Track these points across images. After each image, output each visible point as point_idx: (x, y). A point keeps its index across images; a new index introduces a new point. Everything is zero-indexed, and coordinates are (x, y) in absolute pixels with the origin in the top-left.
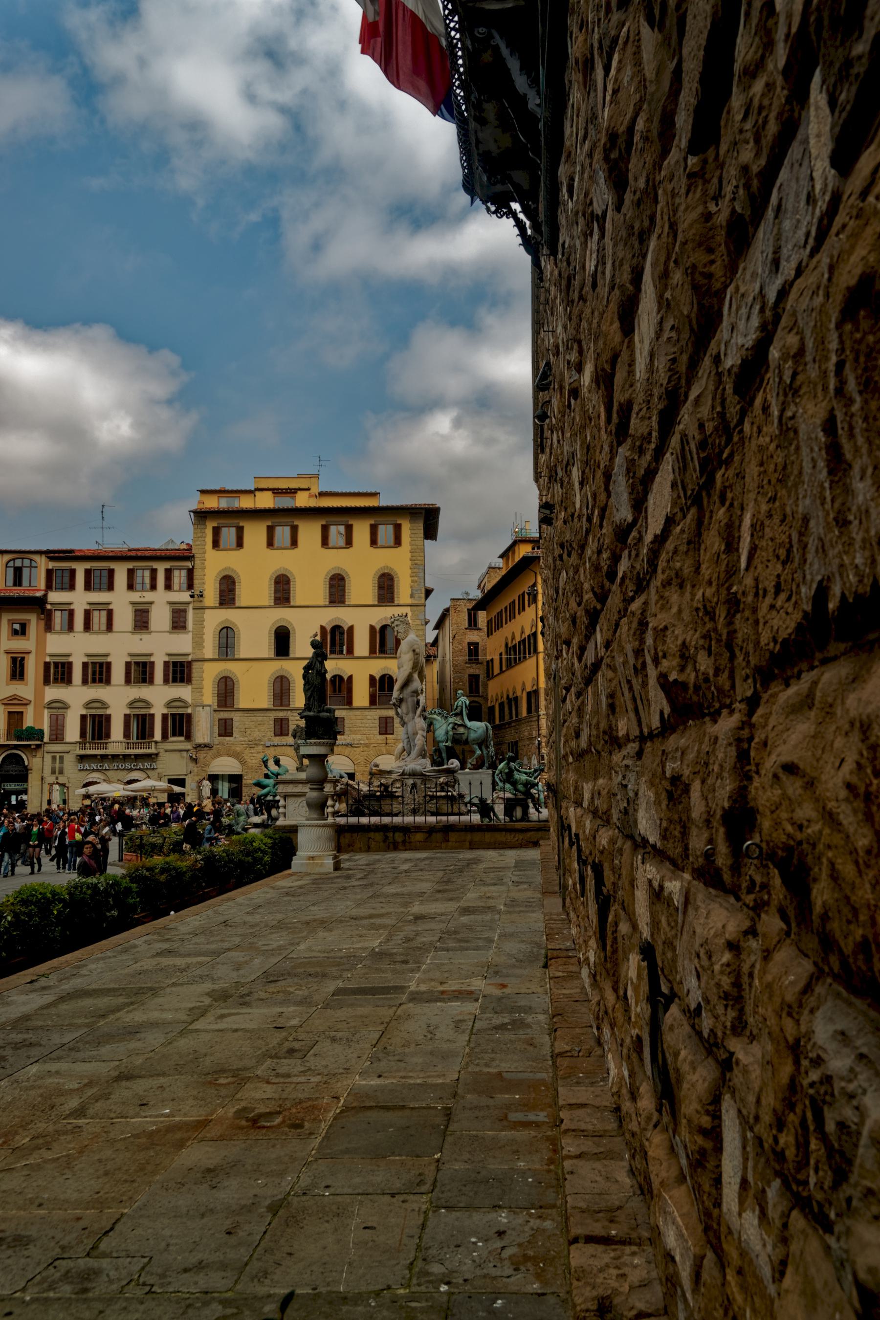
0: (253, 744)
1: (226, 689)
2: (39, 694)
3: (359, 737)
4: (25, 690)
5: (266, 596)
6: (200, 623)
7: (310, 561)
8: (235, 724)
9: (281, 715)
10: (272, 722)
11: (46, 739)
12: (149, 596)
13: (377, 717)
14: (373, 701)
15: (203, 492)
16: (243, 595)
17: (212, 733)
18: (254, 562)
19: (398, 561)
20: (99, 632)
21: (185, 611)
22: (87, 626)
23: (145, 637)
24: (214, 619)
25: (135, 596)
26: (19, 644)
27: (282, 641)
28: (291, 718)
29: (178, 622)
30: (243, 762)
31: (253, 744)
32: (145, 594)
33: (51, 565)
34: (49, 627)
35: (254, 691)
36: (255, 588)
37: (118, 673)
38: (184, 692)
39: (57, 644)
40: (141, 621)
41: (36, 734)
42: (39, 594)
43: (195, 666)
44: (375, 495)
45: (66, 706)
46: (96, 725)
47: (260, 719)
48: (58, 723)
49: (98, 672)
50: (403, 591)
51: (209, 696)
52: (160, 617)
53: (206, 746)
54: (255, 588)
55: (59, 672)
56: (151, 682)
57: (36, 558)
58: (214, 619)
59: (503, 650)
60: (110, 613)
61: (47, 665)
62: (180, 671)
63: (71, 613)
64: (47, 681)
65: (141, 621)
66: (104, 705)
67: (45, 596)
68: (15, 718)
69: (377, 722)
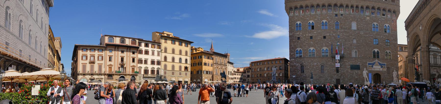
1: (165, 66)
5: (171, 52)
6: (161, 55)
12: (154, 49)
16: (168, 51)
24: (164, 54)
25: (152, 49)
26: (134, 56)
27: (173, 59)
29: (158, 55)
35: (169, 68)
36: (169, 50)
38: (159, 66)
39: (140, 56)
40: (153, 54)
41: (137, 72)
45: (141, 67)
46: (146, 71)
48: (140, 70)
51: (163, 68)
52: (156, 53)
54: (169, 50)
55: (140, 61)
58: (164, 54)
62: (159, 63)
64: (138, 63)
65: (153, 54)
66: (148, 68)
68: (133, 69)
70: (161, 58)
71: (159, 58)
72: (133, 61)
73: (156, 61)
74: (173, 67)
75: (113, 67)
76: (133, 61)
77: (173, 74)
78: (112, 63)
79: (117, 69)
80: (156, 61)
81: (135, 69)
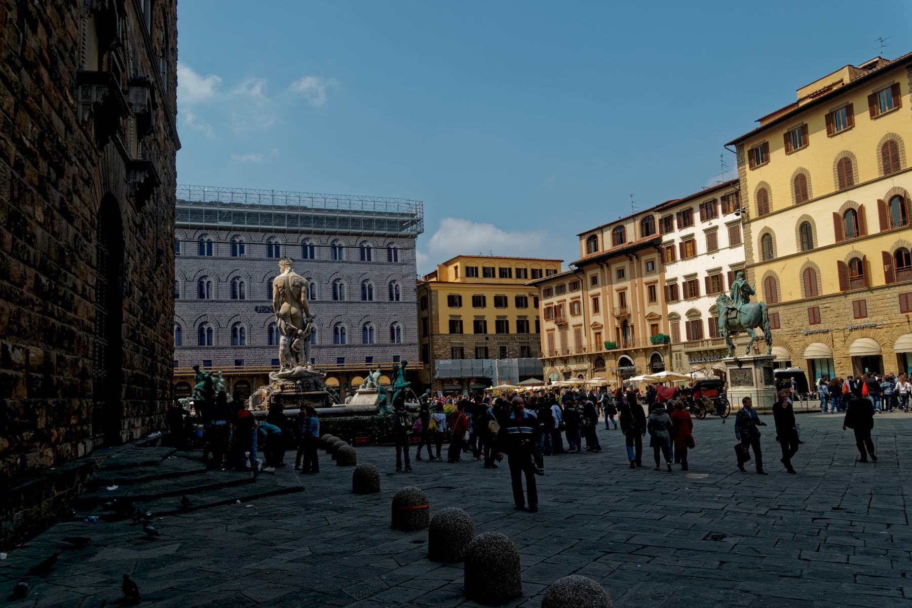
0: (795, 334)
2: (665, 309)
3: (881, 317)
6: (748, 235)
7: (820, 152)
8: (781, 317)
9: (812, 304)
10: (806, 312)
11: (672, 342)
12: (714, 222)
13: (896, 295)
14: (889, 277)
18: (779, 169)
21: (738, 228)
23: (715, 255)
25: (706, 225)
28: (821, 306)
30: (790, 350)
31: (795, 334)
32: (712, 221)
47: (798, 310)
49: (692, 288)
58: (756, 228)
61: (665, 287)
69: (897, 299)
70: (749, 253)
73: (725, 272)
74: (810, 276)
75: (603, 331)
76: (653, 298)
77: (815, 317)
78: (599, 319)
79: (612, 339)
81: (661, 323)
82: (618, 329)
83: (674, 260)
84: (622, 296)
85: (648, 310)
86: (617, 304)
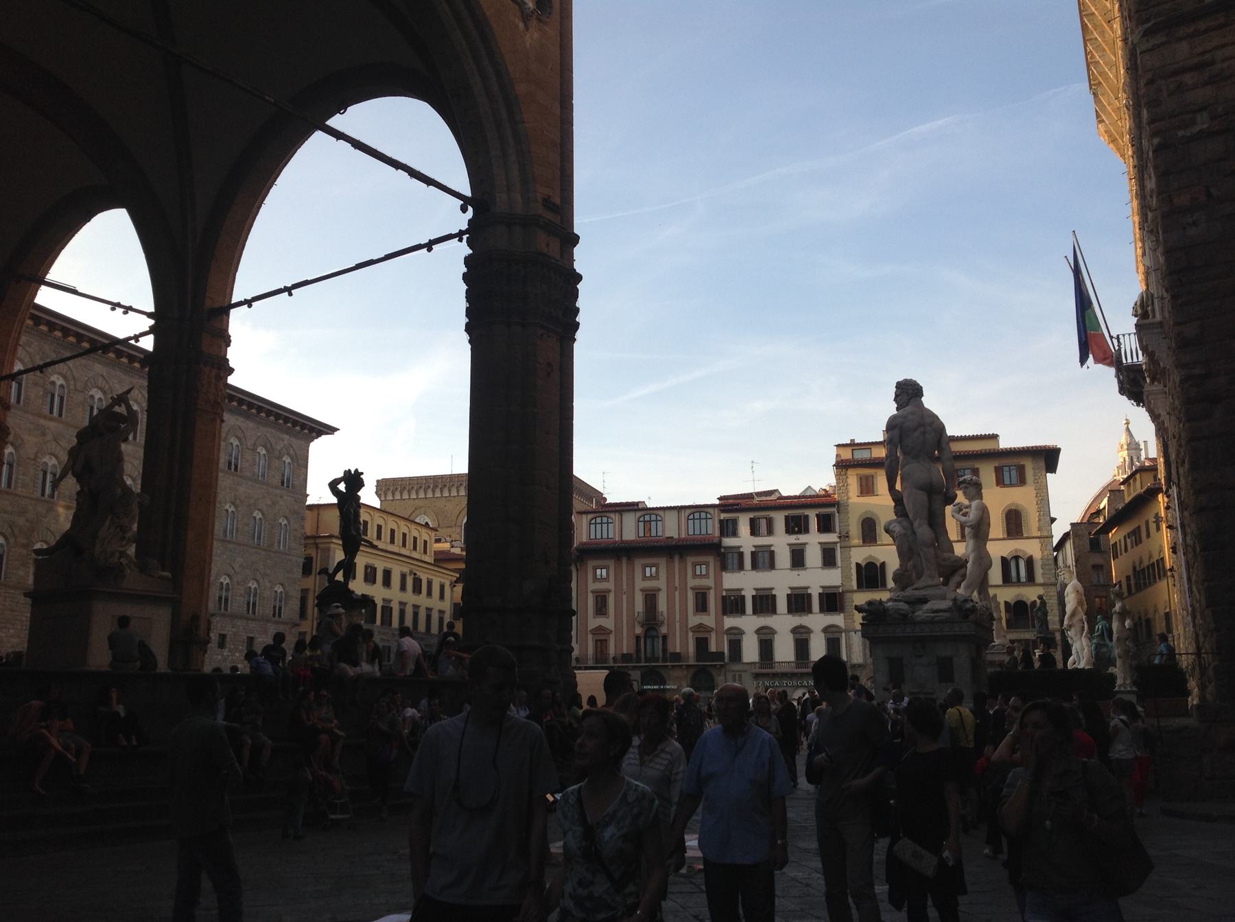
2: (719, 623)
4: (708, 620)
6: (847, 559)
12: (803, 538)
15: (838, 446)
17: (865, 655)
19: (1021, 496)
20: (764, 569)
22: (755, 566)
23: (802, 573)
25: (792, 539)
29: (829, 559)
32: (800, 536)
33: (723, 516)
34: (724, 567)
37: (782, 604)
38: (838, 620)
39: (731, 581)
40: (798, 558)
41: (720, 655)
42: (716, 541)
43: (848, 595)
44: (994, 437)
48: (736, 646)
50: (1032, 522)
52: (813, 556)
53: (860, 666)
55: (733, 604)
56: (810, 611)
57: (711, 510)
59: (1130, 573)
60: (772, 554)
62: (832, 601)
63: (741, 555)
65: (798, 558)
67: (720, 541)
68: (702, 644)
70: (845, 576)
71: (833, 578)
72: (702, 606)
73: (815, 592)
76: (702, 606)
78: (608, 622)
79: (627, 647)
80: (815, 592)
82: (638, 638)
83: (741, 567)
84: (651, 598)
85: (694, 620)
86: (639, 606)
